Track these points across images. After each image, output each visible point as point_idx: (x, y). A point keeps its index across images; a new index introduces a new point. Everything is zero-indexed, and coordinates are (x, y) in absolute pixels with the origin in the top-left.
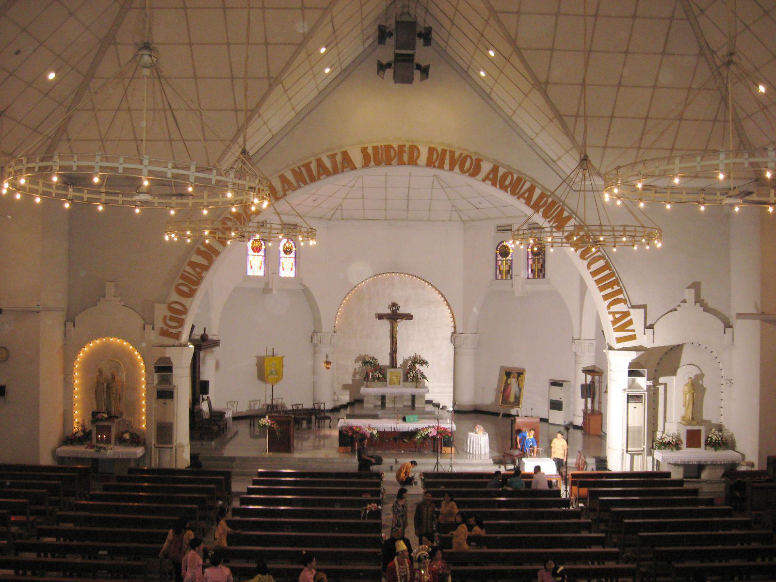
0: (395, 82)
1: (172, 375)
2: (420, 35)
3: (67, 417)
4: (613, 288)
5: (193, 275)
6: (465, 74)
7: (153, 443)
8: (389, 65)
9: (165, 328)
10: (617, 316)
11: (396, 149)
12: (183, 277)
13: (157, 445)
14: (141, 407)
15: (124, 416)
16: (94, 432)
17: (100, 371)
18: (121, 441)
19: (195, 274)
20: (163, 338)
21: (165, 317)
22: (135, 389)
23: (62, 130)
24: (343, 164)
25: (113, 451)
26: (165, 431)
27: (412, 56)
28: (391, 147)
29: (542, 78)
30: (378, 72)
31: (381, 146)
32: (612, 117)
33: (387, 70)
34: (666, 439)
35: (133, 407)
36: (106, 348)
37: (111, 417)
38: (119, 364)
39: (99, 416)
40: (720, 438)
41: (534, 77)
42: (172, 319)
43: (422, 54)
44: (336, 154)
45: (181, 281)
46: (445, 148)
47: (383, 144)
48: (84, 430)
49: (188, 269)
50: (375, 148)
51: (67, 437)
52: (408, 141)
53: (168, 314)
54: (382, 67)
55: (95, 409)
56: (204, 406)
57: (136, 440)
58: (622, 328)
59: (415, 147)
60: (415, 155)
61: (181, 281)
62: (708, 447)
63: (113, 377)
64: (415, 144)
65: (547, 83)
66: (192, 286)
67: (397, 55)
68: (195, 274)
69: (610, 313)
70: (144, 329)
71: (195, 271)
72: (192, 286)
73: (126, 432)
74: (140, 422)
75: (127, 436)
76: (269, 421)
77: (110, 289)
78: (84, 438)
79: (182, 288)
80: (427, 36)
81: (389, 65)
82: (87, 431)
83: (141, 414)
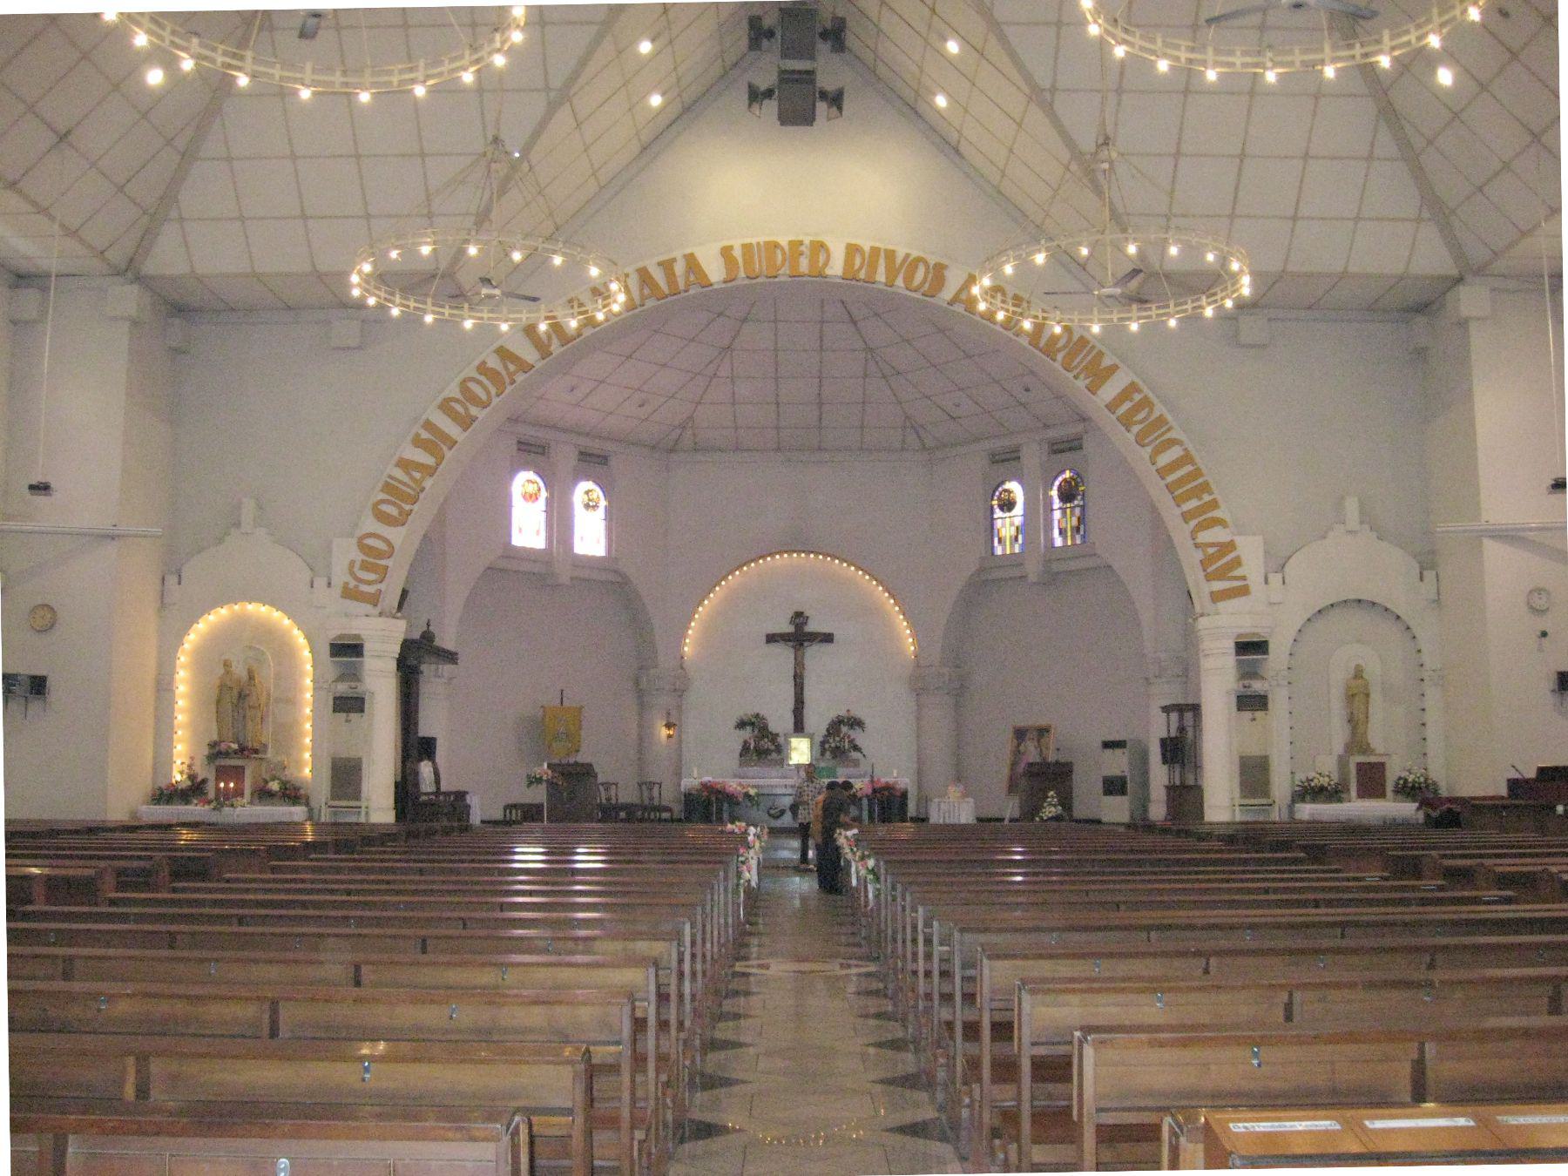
0: (782, 125)
1: (362, 663)
2: (824, 35)
3: (162, 759)
4: (1200, 499)
5: (405, 484)
6: (913, 111)
7: (324, 800)
8: (769, 93)
9: (352, 583)
10: (1211, 551)
11: (787, 248)
12: (387, 488)
13: (329, 804)
14: (302, 734)
15: (270, 754)
16: (211, 776)
17: (227, 664)
18: (263, 794)
19: (411, 484)
20: (348, 602)
21: (352, 563)
22: (291, 701)
23: (169, 197)
24: (687, 278)
25: (246, 811)
26: (346, 776)
27: (811, 73)
28: (776, 245)
29: (1043, 78)
30: (750, 105)
31: (758, 244)
32: (1178, 154)
33: (766, 102)
34: (1316, 781)
35: (288, 734)
36: (242, 622)
37: (243, 751)
38: (263, 653)
39: (223, 747)
40: (1422, 779)
41: (1028, 77)
42: (365, 566)
43: (829, 70)
44: (674, 260)
45: (382, 496)
46: (877, 245)
47: (762, 239)
48: (192, 777)
49: (399, 473)
50: (747, 248)
51: (160, 789)
52: (807, 234)
53: (359, 557)
54: (756, 96)
55: (215, 737)
56: (427, 784)
57: (291, 794)
58: (1221, 575)
59: (822, 245)
60: (822, 259)
61: (382, 496)
62: (1400, 797)
63: (251, 678)
64: (820, 238)
65: (1054, 89)
66: (403, 505)
67: (782, 72)
68: (411, 484)
69: (1197, 546)
70: (312, 587)
71: (412, 478)
72: (403, 505)
73: (273, 779)
74: (299, 764)
75: (275, 786)
76: (550, 772)
77: (249, 510)
78: (194, 790)
79: (384, 507)
80: (836, 35)
81: (769, 93)
82: (199, 779)
83: (301, 749)
